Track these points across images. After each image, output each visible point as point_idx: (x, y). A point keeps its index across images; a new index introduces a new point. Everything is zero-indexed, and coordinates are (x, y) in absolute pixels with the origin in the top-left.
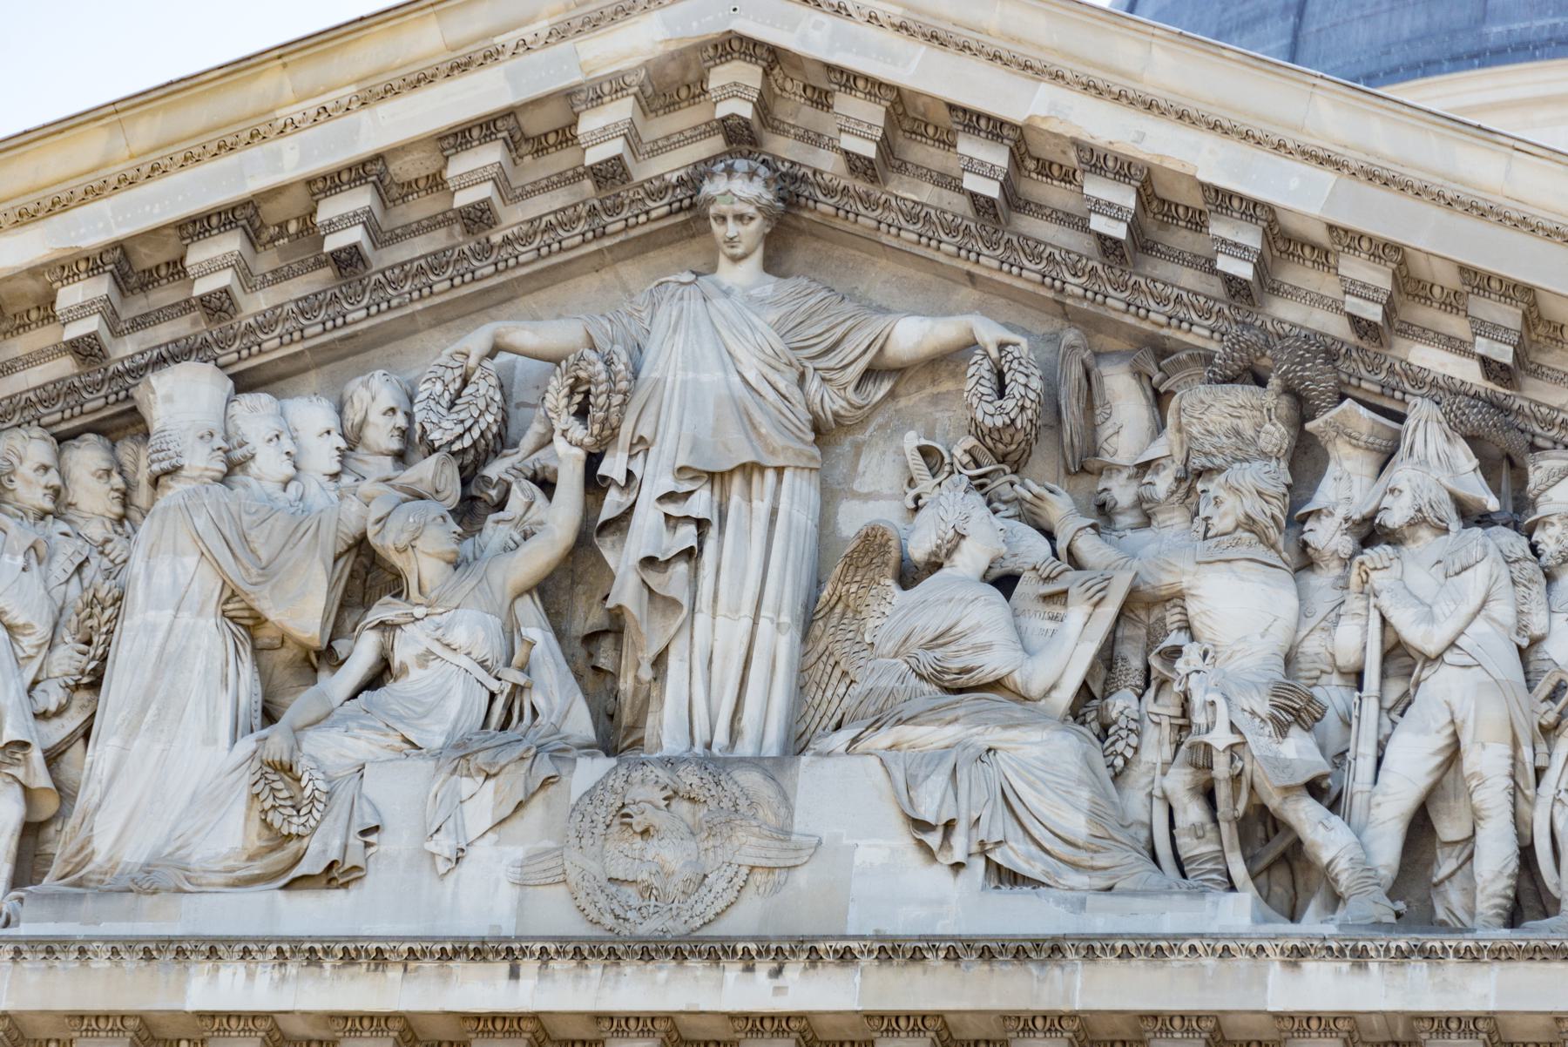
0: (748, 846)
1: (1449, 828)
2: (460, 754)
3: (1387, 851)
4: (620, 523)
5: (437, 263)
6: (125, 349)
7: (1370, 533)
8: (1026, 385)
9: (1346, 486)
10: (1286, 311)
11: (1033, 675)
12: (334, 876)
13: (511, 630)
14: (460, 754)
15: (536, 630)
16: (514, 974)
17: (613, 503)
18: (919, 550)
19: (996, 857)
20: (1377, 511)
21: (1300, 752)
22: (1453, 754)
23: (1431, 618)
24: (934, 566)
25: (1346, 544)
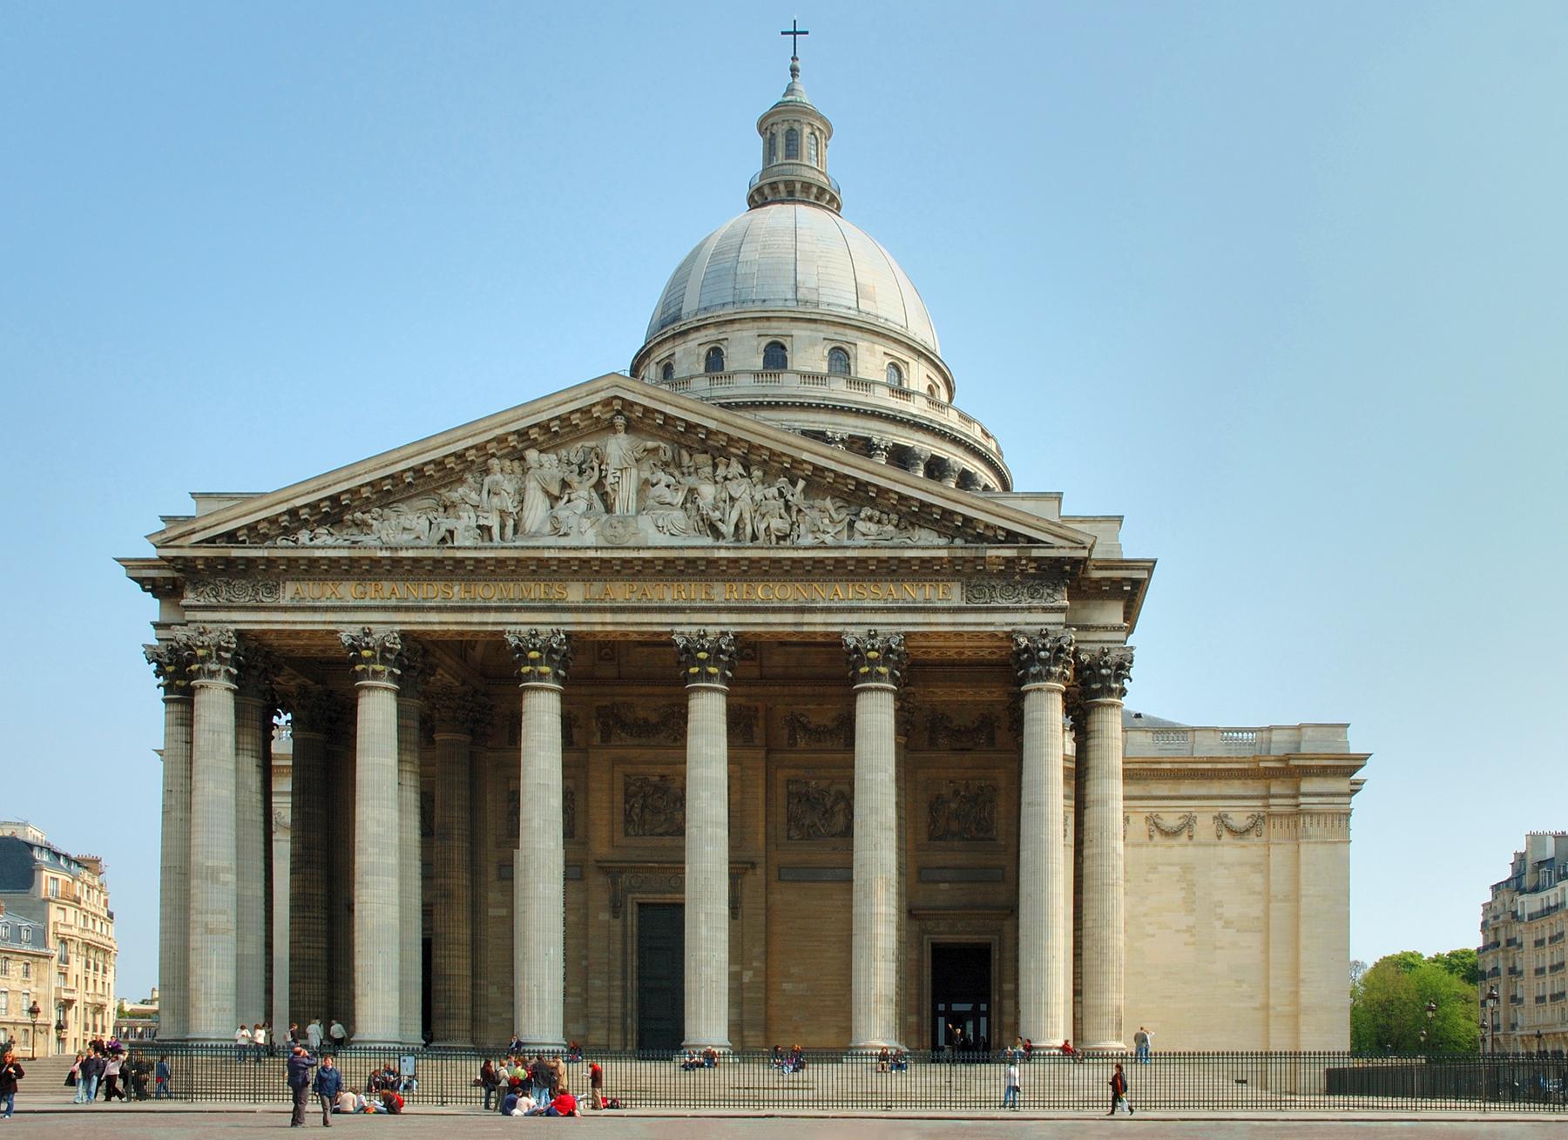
0: (631, 530)
2: (584, 515)
3: (732, 529)
9: (721, 471)
12: (565, 535)
14: (584, 515)
15: (594, 494)
21: (717, 514)
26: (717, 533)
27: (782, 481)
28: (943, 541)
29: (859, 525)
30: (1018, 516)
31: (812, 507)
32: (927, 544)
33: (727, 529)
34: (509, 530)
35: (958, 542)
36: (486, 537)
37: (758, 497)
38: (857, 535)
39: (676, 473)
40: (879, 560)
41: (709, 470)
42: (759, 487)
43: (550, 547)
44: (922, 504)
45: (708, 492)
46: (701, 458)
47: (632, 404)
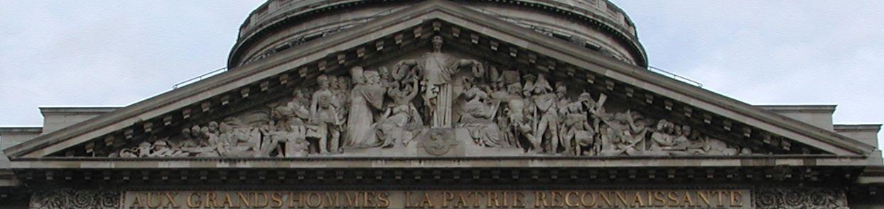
0: (450, 142)
1: (548, 137)
2: (407, 128)
3: (540, 140)
4: (425, 91)
5: (392, 51)
6: (346, 64)
7: (533, 93)
8: (482, 70)
9: (529, 87)
10: (520, 60)
11: (488, 115)
12: (390, 146)
13: (409, 107)
16: (420, 162)
17: (423, 89)
18: (470, 95)
19: (487, 143)
20: (534, 90)
21: (527, 127)
22: (548, 127)
23: (544, 106)
24: (472, 98)
25: (529, 95)
26: (526, 144)
27: (585, 95)
28: (731, 152)
29: (657, 136)
30: (803, 128)
31: (612, 120)
32: (717, 154)
33: (536, 140)
34: (335, 142)
35: (746, 152)
36: (313, 148)
37: (563, 110)
38: (654, 146)
39: (488, 88)
40: (677, 169)
41: (518, 85)
42: (564, 101)
43: (378, 157)
44: (715, 117)
45: (517, 104)
46: (510, 75)
47: (447, 26)
